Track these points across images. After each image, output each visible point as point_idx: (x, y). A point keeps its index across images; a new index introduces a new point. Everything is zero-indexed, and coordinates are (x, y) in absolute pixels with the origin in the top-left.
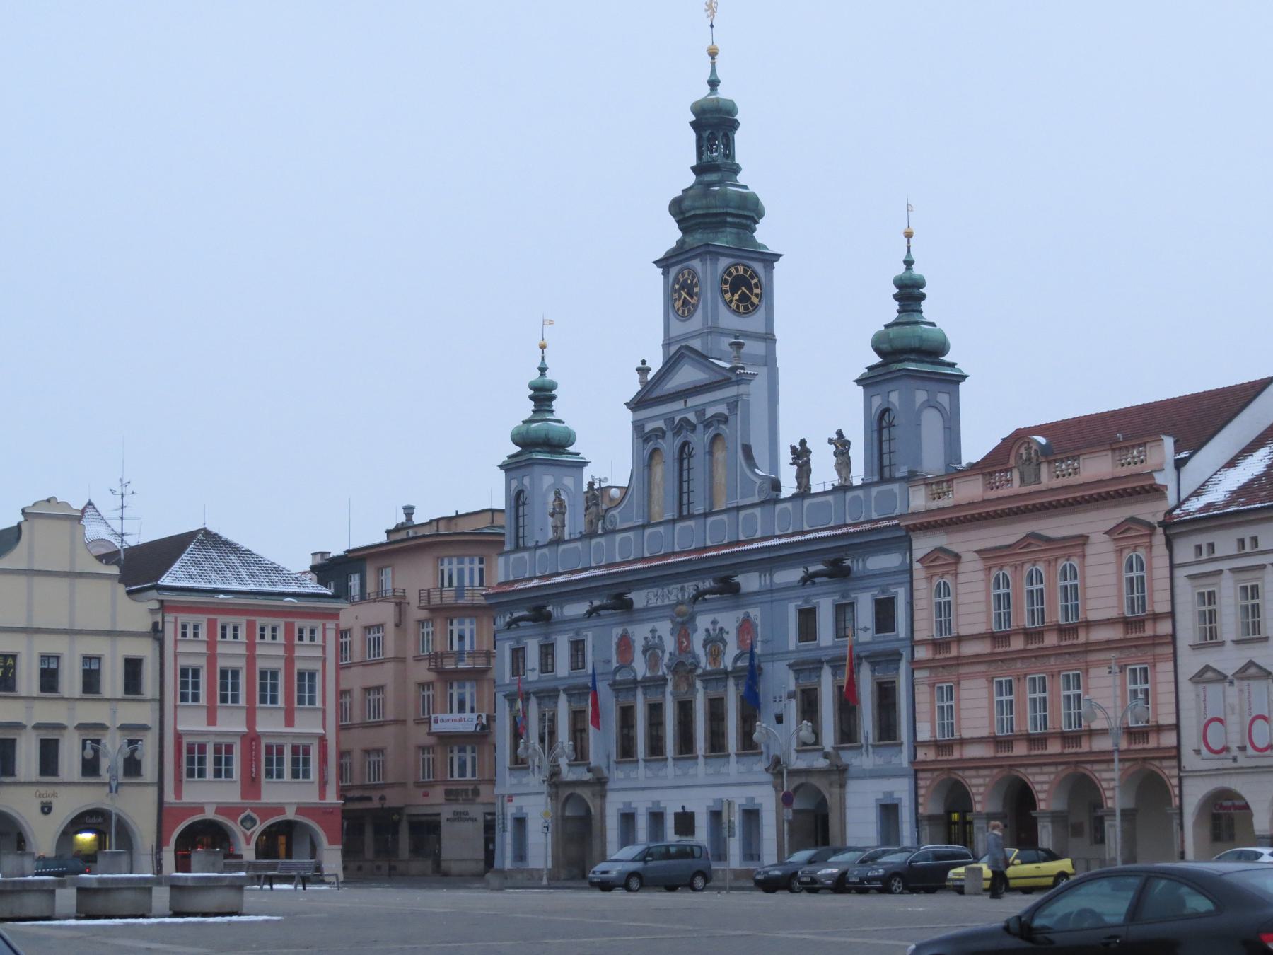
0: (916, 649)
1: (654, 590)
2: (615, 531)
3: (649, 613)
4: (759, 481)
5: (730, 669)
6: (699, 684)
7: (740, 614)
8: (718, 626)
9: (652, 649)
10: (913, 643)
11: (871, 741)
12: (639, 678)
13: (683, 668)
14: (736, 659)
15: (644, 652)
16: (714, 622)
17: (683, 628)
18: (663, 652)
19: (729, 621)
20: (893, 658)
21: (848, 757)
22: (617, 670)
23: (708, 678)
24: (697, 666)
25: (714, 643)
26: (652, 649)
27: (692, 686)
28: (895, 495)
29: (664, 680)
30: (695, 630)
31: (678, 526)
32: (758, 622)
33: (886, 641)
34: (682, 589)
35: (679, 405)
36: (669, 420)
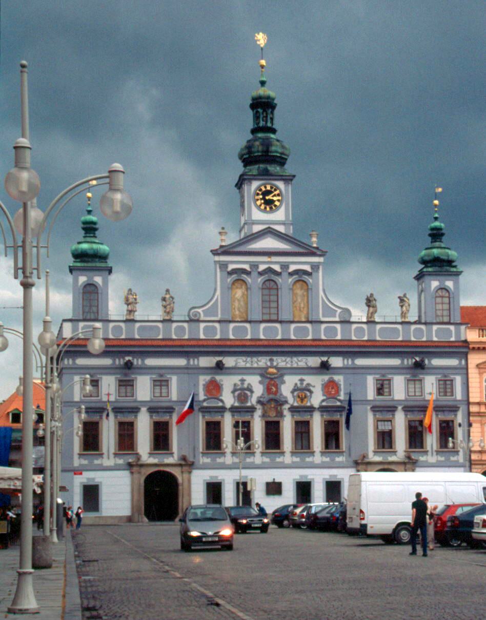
0: (471, 406)
1: (244, 358)
2: (198, 321)
3: (235, 370)
4: (339, 311)
5: (316, 405)
6: (286, 413)
7: (326, 378)
8: (305, 383)
9: (242, 393)
10: (469, 404)
11: (435, 448)
12: (228, 406)
13: (273, 402)
14: (323, 401)
15: (233, 392)
16: (302, 380)
17: (272, 381)
18: (252, 392)
19: (316, 382)
20: (454, 409)
21: (414, 456)
22: (204, 400)
23: (293, 410)
24: (286, 402)
25: (303, 392)
26: (242, 393)
27: (281, 414)
28: (451, 331)
29: (252, 410)
30: (283, 382)
31: (263, 325)
32: (342, 383)
33: (446, 400)
34: (271, 360)
35: (265, 259)
36: (255, 266)
